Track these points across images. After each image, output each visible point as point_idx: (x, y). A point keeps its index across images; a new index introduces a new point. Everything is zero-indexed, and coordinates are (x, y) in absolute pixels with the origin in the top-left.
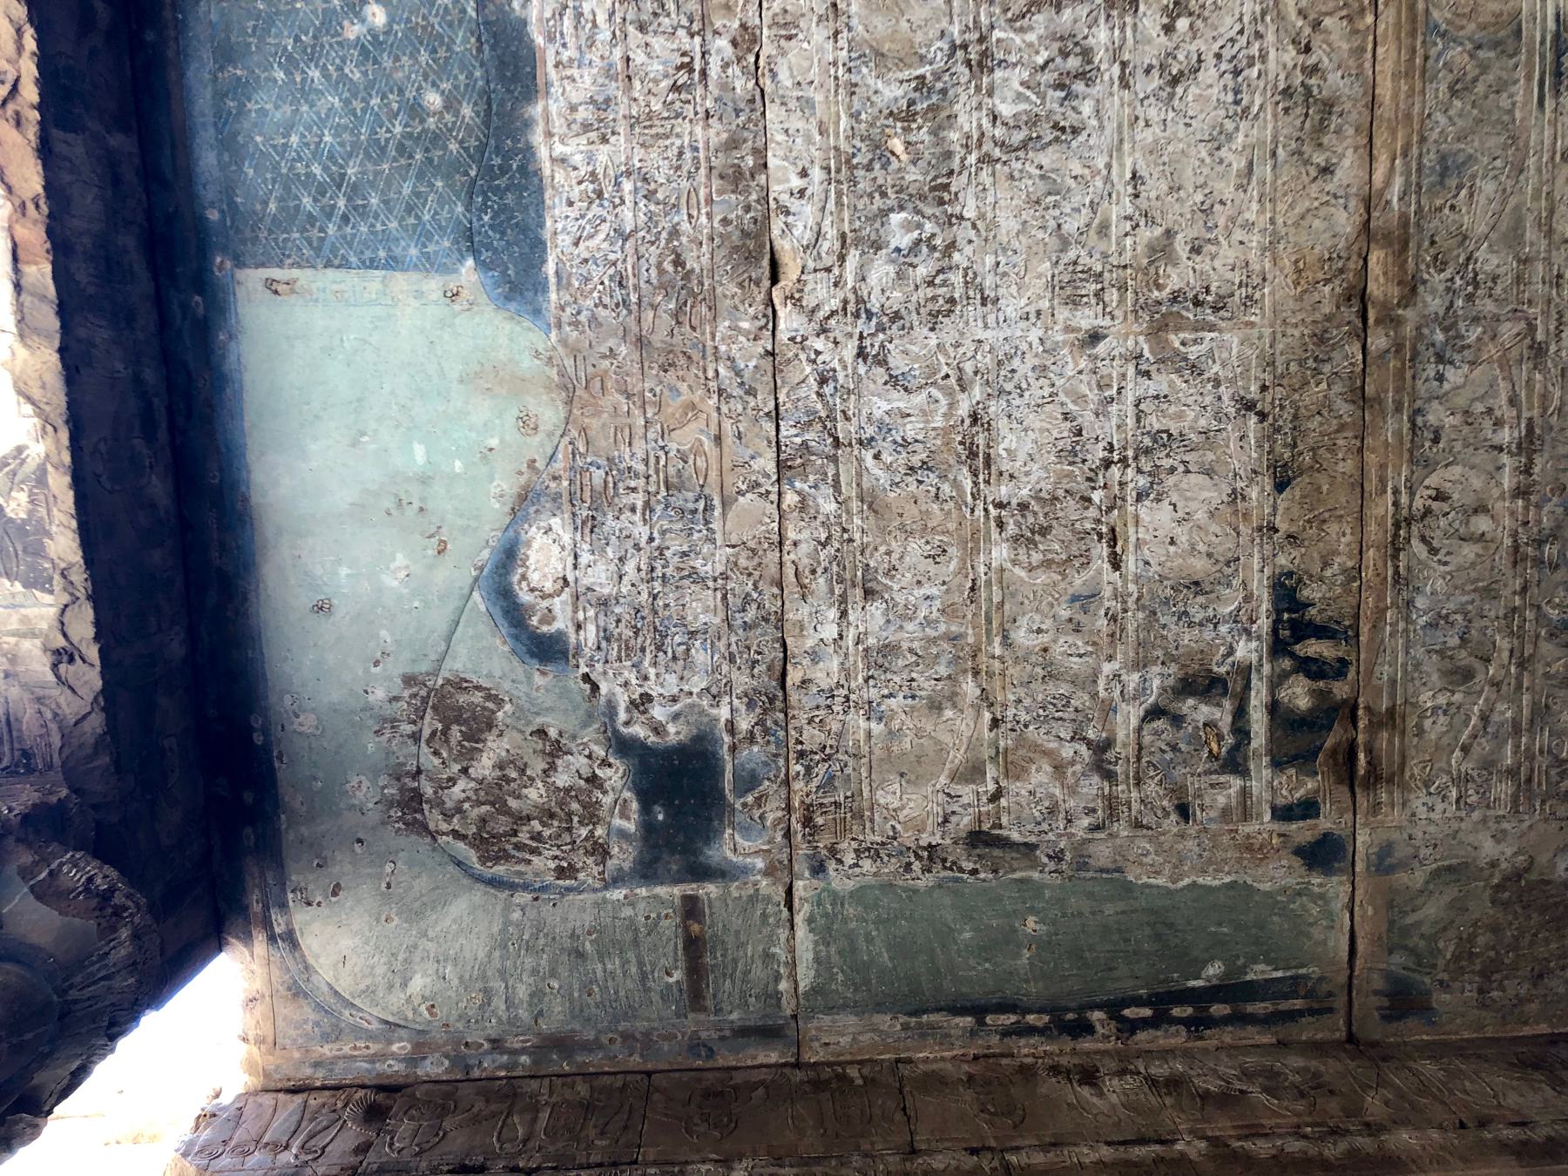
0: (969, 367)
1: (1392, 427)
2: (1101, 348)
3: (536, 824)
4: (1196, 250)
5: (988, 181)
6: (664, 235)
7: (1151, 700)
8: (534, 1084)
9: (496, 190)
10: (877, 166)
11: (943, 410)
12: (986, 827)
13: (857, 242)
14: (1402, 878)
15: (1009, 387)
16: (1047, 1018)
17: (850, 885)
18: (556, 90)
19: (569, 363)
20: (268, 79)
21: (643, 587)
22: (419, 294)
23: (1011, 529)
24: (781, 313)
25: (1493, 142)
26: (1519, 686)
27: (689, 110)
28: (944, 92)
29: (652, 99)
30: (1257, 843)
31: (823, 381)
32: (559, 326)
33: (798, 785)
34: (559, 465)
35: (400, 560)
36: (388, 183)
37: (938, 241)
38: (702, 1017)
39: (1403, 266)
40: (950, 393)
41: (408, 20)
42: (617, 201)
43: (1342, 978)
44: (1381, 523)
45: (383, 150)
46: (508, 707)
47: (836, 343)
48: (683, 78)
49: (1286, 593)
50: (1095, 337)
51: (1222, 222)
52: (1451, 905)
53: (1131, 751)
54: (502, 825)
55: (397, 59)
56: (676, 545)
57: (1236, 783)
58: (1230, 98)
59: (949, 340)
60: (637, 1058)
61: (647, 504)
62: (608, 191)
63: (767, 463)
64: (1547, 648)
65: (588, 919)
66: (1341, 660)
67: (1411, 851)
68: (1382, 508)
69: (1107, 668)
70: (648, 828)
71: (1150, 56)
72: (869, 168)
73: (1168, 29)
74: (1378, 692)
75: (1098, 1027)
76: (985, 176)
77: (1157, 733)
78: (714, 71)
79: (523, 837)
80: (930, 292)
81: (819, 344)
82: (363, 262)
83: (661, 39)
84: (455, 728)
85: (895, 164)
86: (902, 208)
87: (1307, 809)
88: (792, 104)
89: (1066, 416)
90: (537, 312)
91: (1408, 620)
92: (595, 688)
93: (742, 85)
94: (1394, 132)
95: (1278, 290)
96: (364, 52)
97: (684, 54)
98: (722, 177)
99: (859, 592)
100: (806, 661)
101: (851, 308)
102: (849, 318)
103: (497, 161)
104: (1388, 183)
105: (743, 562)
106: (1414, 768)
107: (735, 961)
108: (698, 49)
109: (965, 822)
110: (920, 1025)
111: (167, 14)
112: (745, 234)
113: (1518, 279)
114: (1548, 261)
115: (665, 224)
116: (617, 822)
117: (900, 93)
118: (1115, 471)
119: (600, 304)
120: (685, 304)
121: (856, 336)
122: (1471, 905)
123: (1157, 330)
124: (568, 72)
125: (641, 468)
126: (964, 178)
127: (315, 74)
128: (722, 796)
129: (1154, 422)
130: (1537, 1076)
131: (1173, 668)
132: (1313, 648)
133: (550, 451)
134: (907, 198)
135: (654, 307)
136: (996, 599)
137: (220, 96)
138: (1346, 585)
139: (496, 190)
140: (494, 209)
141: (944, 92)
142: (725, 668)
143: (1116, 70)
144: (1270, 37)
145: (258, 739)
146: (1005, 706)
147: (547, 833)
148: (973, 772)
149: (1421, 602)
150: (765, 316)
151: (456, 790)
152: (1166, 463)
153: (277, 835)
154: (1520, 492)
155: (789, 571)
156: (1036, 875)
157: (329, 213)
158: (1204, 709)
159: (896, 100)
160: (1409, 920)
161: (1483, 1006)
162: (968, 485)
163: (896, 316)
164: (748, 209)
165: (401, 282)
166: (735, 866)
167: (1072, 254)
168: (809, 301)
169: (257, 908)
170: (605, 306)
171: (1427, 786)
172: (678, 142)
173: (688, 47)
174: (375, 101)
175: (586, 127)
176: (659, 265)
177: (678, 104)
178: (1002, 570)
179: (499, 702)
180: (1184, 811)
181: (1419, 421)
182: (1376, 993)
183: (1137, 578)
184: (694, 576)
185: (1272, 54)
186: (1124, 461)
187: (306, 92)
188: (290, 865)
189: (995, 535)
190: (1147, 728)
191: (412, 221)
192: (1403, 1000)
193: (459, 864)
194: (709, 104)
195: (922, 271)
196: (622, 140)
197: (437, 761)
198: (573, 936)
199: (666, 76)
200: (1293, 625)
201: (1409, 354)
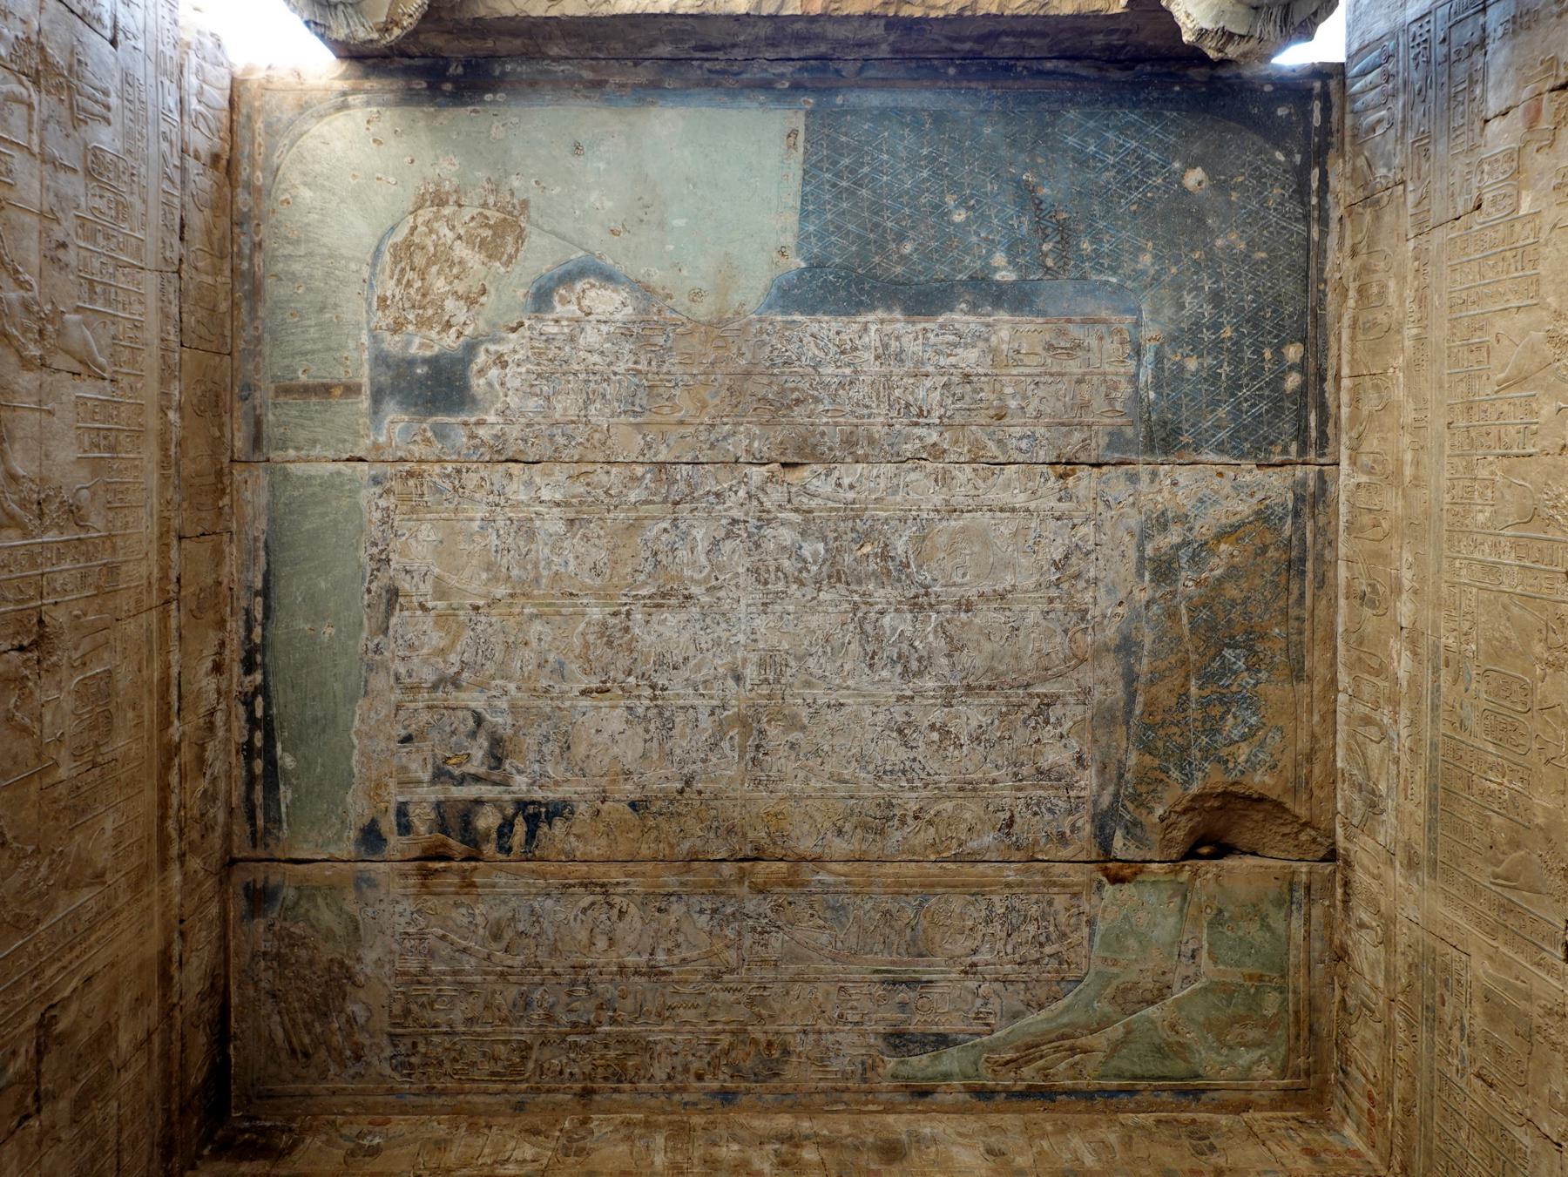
0: (722, 594)
1: (671, 880)
2: (731, 683)
3: (419, 284)
4: (792, 746)
5: (842, 608)
7: (488, 717)
8: (227, 273)
9: (848, 285)
11: (697, 576)
12: (401, 600)
13: (806, 521)
14: (351, 895)
15: (708, 620)
16: (258, 641)
17: (364, 503)
18: (910, 328)
19: (736, 325)
21: (582, 367)
22: (784, 230)
23: (612, 621)
24: (764, 469)
25: (853, 940)
26: (487, 973)
28: (899, 580)
30: (382, 792)
31: (717, 495)
32: (760, 321)
33: (437, 468)
34: (668, 314)
35: (608, 204)
36: (856, 215)
37: (805, 574)
38: (272, 394)
39: (777, 884)
40: (706, 580)
43: (278, 854)
44: (605, 874)
45: (876, 213)
46: (502, 270)
48: (914, 410)
49: (558, 810)
50: (738, 678)
51: (810, 763)
52: (329, 930)
53: (452, 703)
54: (419, 260)
56: (610, 390)
57: (426, 776)
58: (888, 768)
59: (741, 581)
60: (242, 345)
61: (640, 372)
64: (513, 992)
65: (347, 317)
66: (509, 850)
67: (371, 901)
68: (615, 874)
69: (512, 687)
70: (412, 362)
71: (916, 715)
72: (853, 530)
73: (932, 727)
74: (488, 876)
75: (249, 678)
76: (845, 606)
77: (464, 720)
78: (917, 431)
79: (410, 275)
80: (772, 568)
81: (742, 493)
84: (490, 233)
86: (827, 551)
87: (405, 828)
89: (686, 659)
91: (537, 894)
92: (514, 330)
93: (908, 449)
94: (862, 875)
95: (765, 800)
96: (937, 207)
99: (572, 515)
100: (525, 477)
101: (765, 515)
104: (830, 872)
105: (597, 436)
106: (432, 902)
107: (312, 419)
109: (405, 585)
110: (257, 550)
111: (965, 84)
113: (764, 961)
114: (775, 980)
115: (823, 394)
116: (417, 341)
118: (648, 692)
119: (774, 348)
122: (330, 945)
123: (743, 722)
125: (664, 369)
126: (844, 592)
128: (431, 414)
129: (680, 718)
130: (208, 985)
131: (510, 732)
132: (520, 828)
134: (833, 555)
135: (770, 384)
136: (564, 611)
137: (914, 112)
138: (563, 851)
139: (848, 285)
140: (838, 280)
141: (899, 580)
142: (523, 420)
143: (908, 693)
144: (924, 793)
145: (488, 97)
146: (488, 615)
147: (412, 291)
148: (441, 592)
149: (549, 903)
151: (446, 231)
152: (652, 727)
153: (419, 104)
154: (622, 969)
155: (589, 468)
156: (365, 635)
158: (480, 754)
160: (320, 901)
161: (253, 956)
162: (643, 592)
163: (758, 546)
164: (831, 449)
165: (792, 219)
166: (381, 422)
167: (793, 663)
168: (770, 488)
169: (367, 85)
171: (419, 911)
176: (796, 389)
178: (584, 615)
179: (507, 264)
180: (407, 739)
181: (673, 899)
182: (266, 879)
183: (574, 707)
184: (587, 403)
185: (914, 795)
186: (655, 698)
187: (913, 167)
188: (398, 111)
189: (608, 610)
190: (468, 714)
192: (259, 898)
193: (393, 229)
194: (897, 426)
195: (786, 563)
197: (467, 218)
198: (336, 305)
200: (536, 816)
201: (717, 890)
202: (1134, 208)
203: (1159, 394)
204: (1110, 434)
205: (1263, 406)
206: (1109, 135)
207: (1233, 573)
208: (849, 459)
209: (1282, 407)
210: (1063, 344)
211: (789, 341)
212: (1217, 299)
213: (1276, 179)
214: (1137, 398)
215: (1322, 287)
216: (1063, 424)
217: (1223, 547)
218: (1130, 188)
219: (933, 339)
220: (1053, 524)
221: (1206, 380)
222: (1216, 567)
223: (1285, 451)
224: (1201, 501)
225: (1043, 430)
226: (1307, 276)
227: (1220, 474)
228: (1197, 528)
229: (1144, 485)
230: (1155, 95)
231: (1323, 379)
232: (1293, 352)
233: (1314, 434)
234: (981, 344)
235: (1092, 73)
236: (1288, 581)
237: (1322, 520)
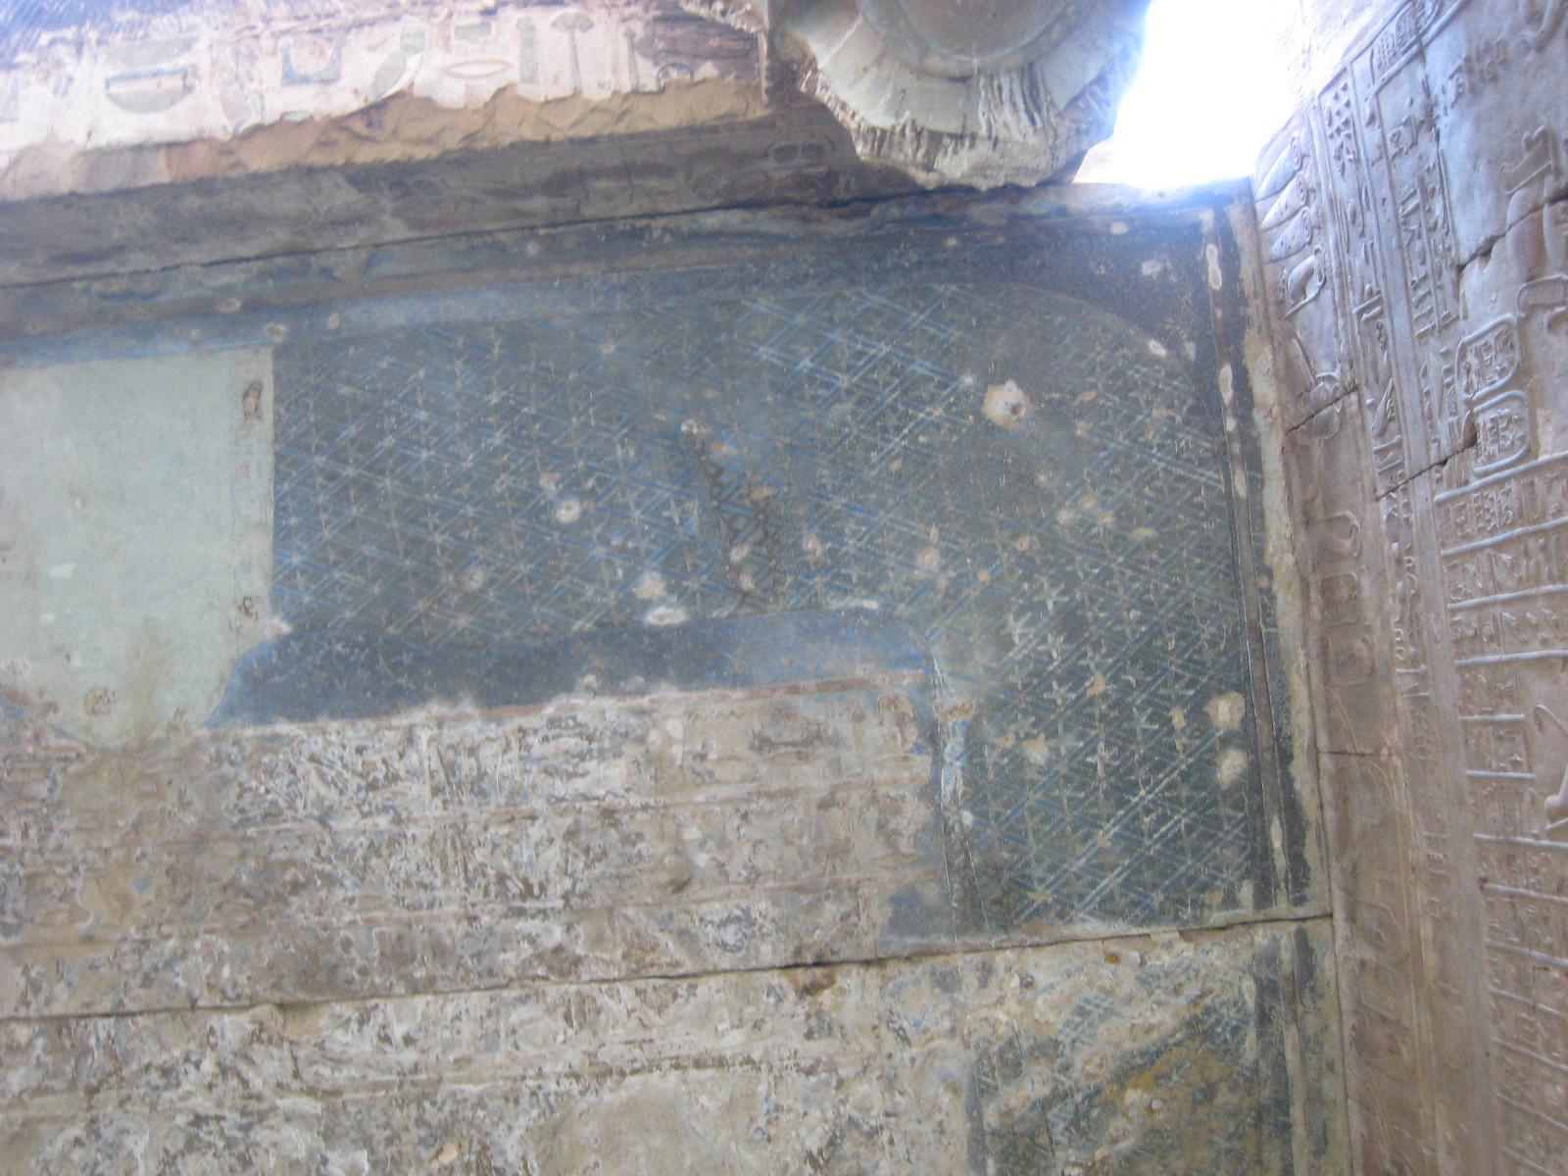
6: (328, 868)
10: (423, 1132)
13: (332, 1111)
18: (493, 730)
20: (490, 383)
22: (247, 568)
27: (475, 895)
29: (490, 847)
31: (166, 1072)
34: (53, 741)
41: (564, 550)
42: (366, 808)
47: (210, 1086)
48: (515, 887)
55: (520, 536)
62: (377, 798)
63: (63, 1003)
72: (420, 1122)
78: (524, 925)
81: (208, 1066)
82: (282, 499)
83: (559, 859)
85: (426, 1154)
86: (374, 1165)
88: (489, 1024)
90: (230, 711)
93: (510, 960)
96: (525, 497)
97: (543, 888)
98: (400, 938)
101: (253, 1105)
102: (240, 1103)
103: (406, 659)
108: (549, 905)
111: (558, 269)
112: (334, 969)
115: (342, 870)
117: (511, 1156)
119: (244, 790)
120: (248, 896)
121: (219, 1112)
124: (514, 745)
125: (52, 843)
127: (498, 439)
133: (69, 729)
135: (243, 855)
140: (344, 655)
150: (238, 997)
157: (339, 456)
159: (503, 1153)
164: (363, 972)
165: (260, 546)
170: (240, 796)
172: (438, 883)
173: (551, 891)
174: (470, 510)
175: (450, 768)
176: (285, 865)
177: (483, 882)
191: (332, 556)
194: (486, 919)
196: (437, 813)
199: (516, 866)
202: (896, 466)
203: (981, 815)
204: (895, 901)
205: (1182, 819)
206: (836, 336)
207: (1155, 1143)
208: (400, 989)
209: (1216, 817)
210: (786, 736)
211: (271, 773)
212: (1071, 623)
213: (1156, 391)
214: (940, 825)
215: (1264, 582)
216: (800, 889)
217: (1132, 1096)
218: (885, 430)
219: (538, 749)
220: (798, 1082)
221: (1067, 779)
222: (1122, 1134)
223: (1230, 901)
224: (1081, 1012)
225: (763, 905)
226: (1233, 566)
227: (1114, 958)
228: (1078, 1065)
229: (968, 991)
230: (915, 258)
231: (1286, 757)
232: (1225, 711)
233: (1281, 862)
234: (630, 750)
235: (791, 228)
236: (1259, 1149)
237: (1312, 1024)
